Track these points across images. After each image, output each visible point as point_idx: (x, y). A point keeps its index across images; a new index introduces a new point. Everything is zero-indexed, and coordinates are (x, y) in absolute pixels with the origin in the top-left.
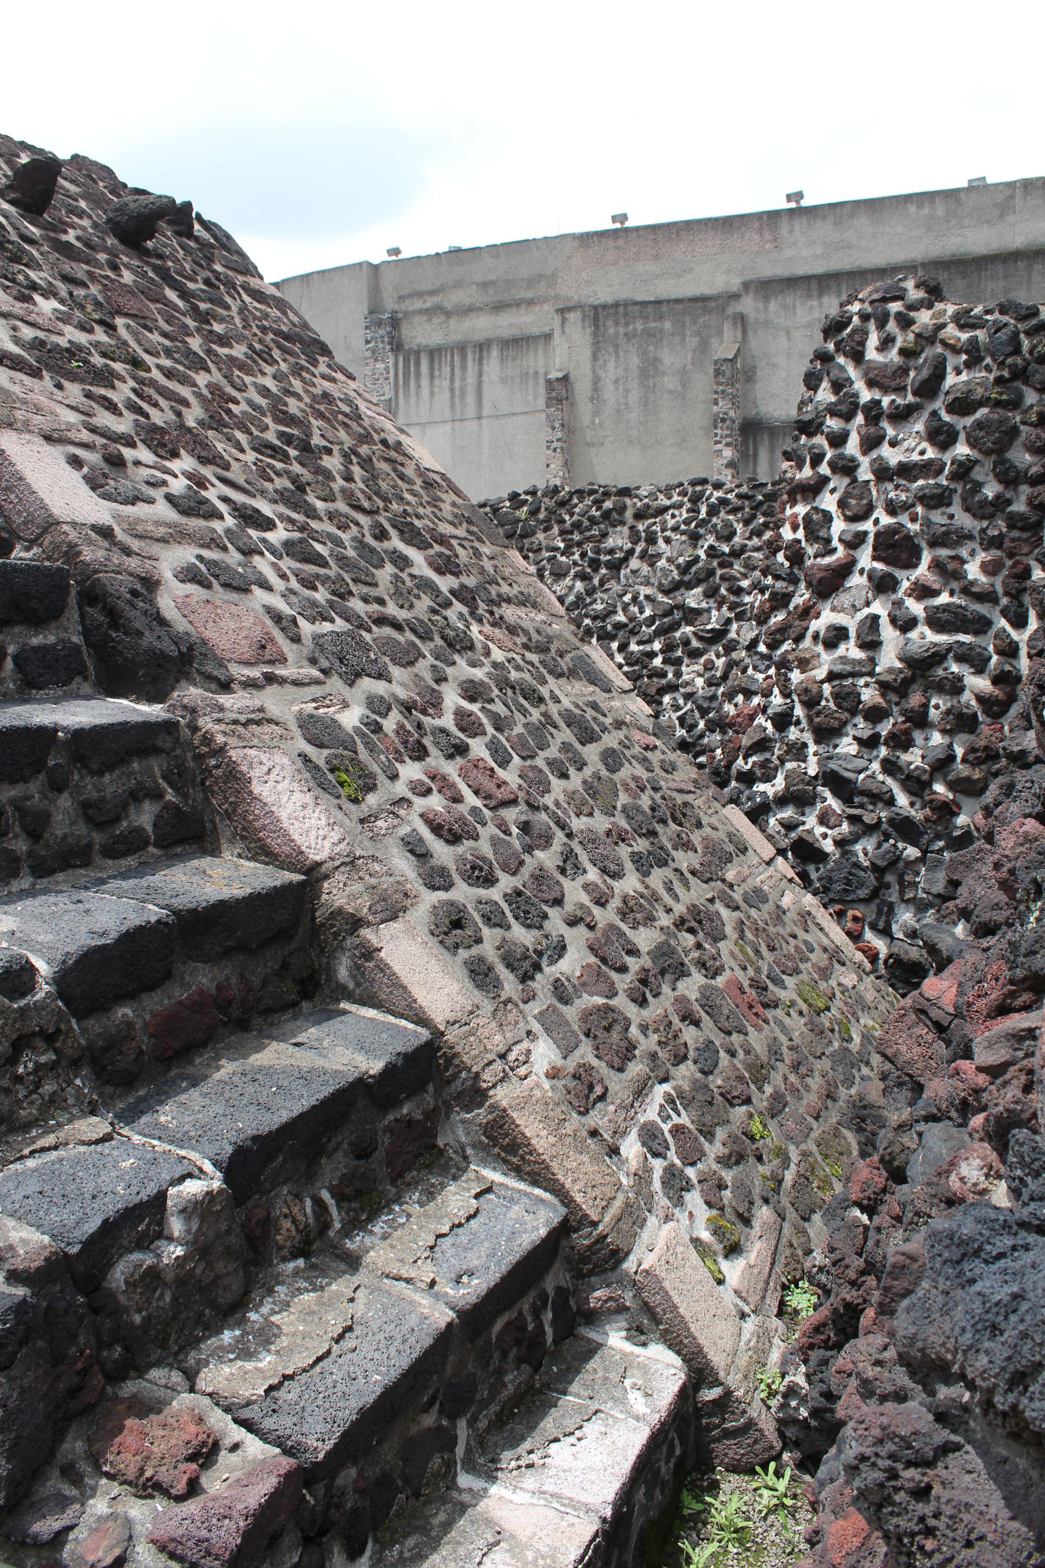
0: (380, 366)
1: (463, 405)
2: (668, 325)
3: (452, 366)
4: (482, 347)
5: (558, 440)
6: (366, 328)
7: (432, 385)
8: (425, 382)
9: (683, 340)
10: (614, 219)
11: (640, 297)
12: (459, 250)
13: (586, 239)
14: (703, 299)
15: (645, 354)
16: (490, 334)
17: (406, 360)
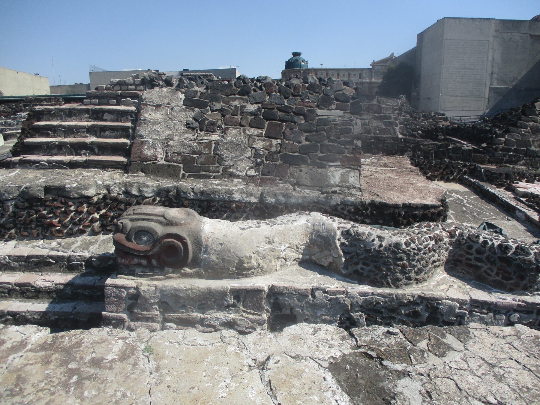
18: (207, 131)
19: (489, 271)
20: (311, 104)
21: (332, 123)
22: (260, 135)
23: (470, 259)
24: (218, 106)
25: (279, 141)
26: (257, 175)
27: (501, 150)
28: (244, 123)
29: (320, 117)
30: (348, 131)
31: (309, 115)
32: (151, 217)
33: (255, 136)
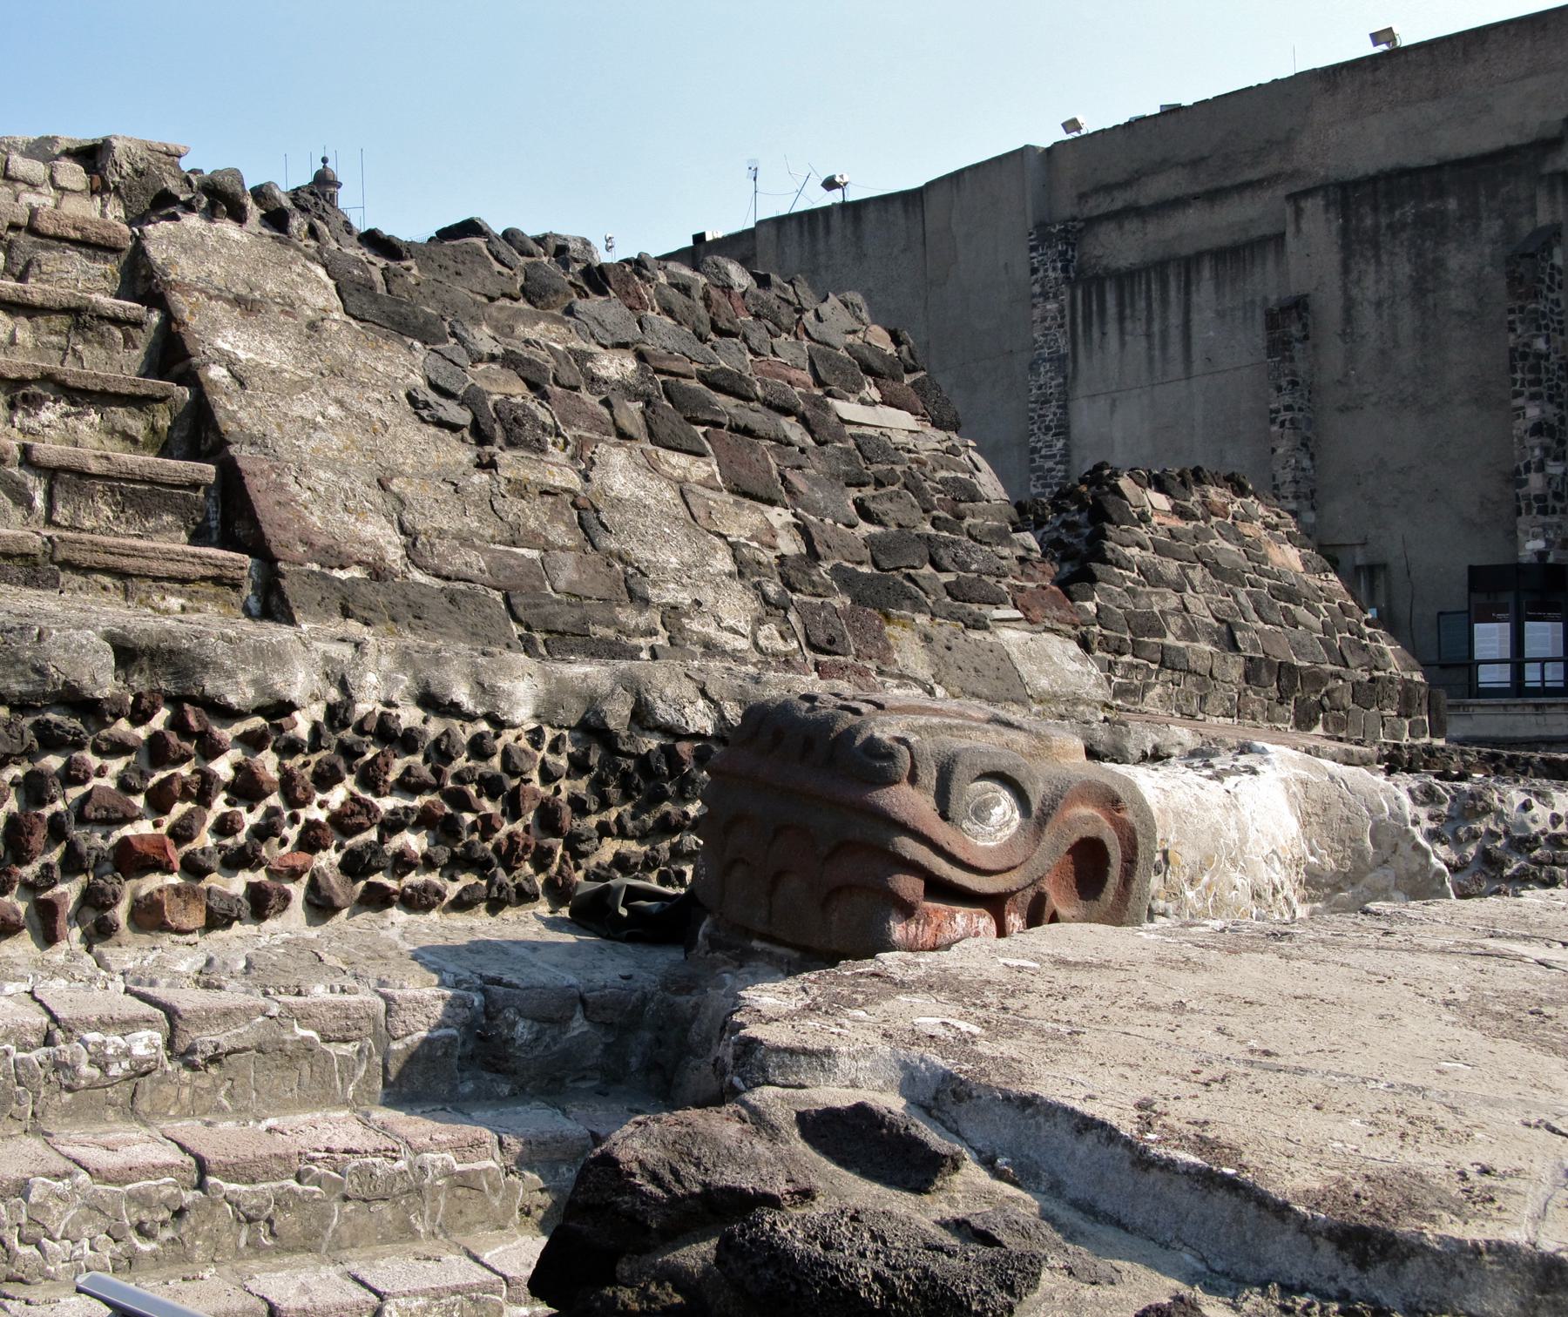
0: (1052, 306)
1: (1165, 359)
2: (1452, 204)
3: (1149, 298)
4: (1189, 265)
5: (1288, 408)
6: (1033, 249)
7: (1122, 332)
8: (1112, 328)
9: (1477, 226)
10: (1376, 38)
11: (1414, 161)
12: (1176, 109)
13: (1331, 76)
14: (1507, 152)
15: (1419, 255)
16: (1205, 246)
21: (906, 455)
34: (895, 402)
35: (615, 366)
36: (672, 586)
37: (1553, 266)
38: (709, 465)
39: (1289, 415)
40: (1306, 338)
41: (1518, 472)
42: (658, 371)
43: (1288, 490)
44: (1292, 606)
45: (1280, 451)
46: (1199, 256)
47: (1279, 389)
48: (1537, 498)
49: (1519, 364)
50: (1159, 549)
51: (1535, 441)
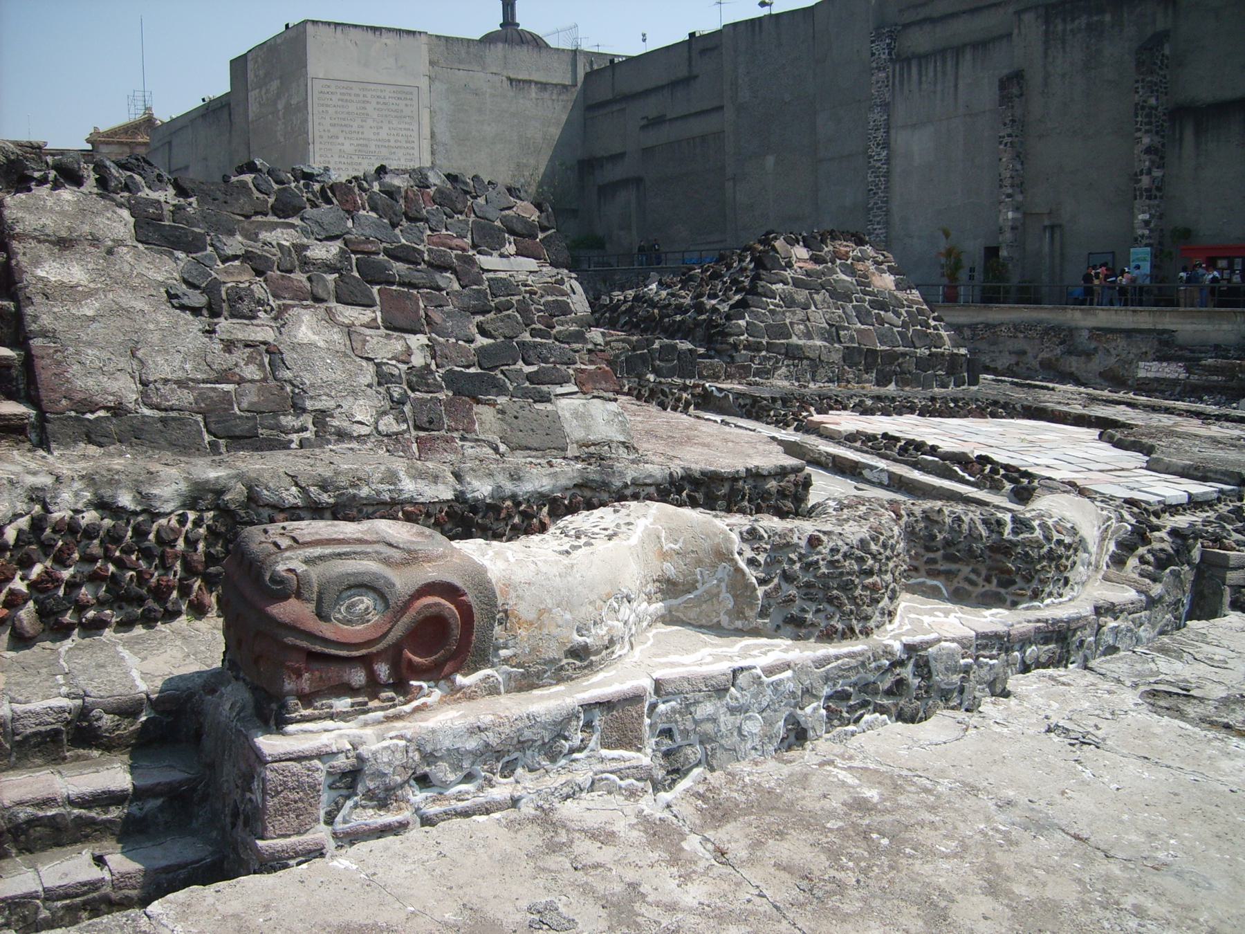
2: (1108, 18)
4: (958, 51)
5: (1009, 136)
6: (873, 42)
15: (1087, 48)
17: (902, 69)
18: (233, 316)
19: (973, 577)
20: (458, 242)
21: (523, 289)
22: (372, 325)
23: (934, 561)
24: (235, 244)
25: (423, 339)
26: (405, 431)
27: (745, 348)
28: (321, 293)
29: (491, 275)
30: (564, 309)
31: (466, 271)
32: (358, 548)
33: (361, 325)
34: (524, 253)
35: (323, 252)
36: (324, 397)
37: (1163, 55)
38: (374, 312)
39: (1010, 139)
40: (1022, 95)
41: (1136, 174)
42: (355, 252)
43: (1008, 182)
44: (882, 313)
45: (1004, 160)
46: (965, 46)
47: (1005, 124)
48: (1146, 190)
49: (1140, 112)
50: (797, 283)
51: (1146, 157)
